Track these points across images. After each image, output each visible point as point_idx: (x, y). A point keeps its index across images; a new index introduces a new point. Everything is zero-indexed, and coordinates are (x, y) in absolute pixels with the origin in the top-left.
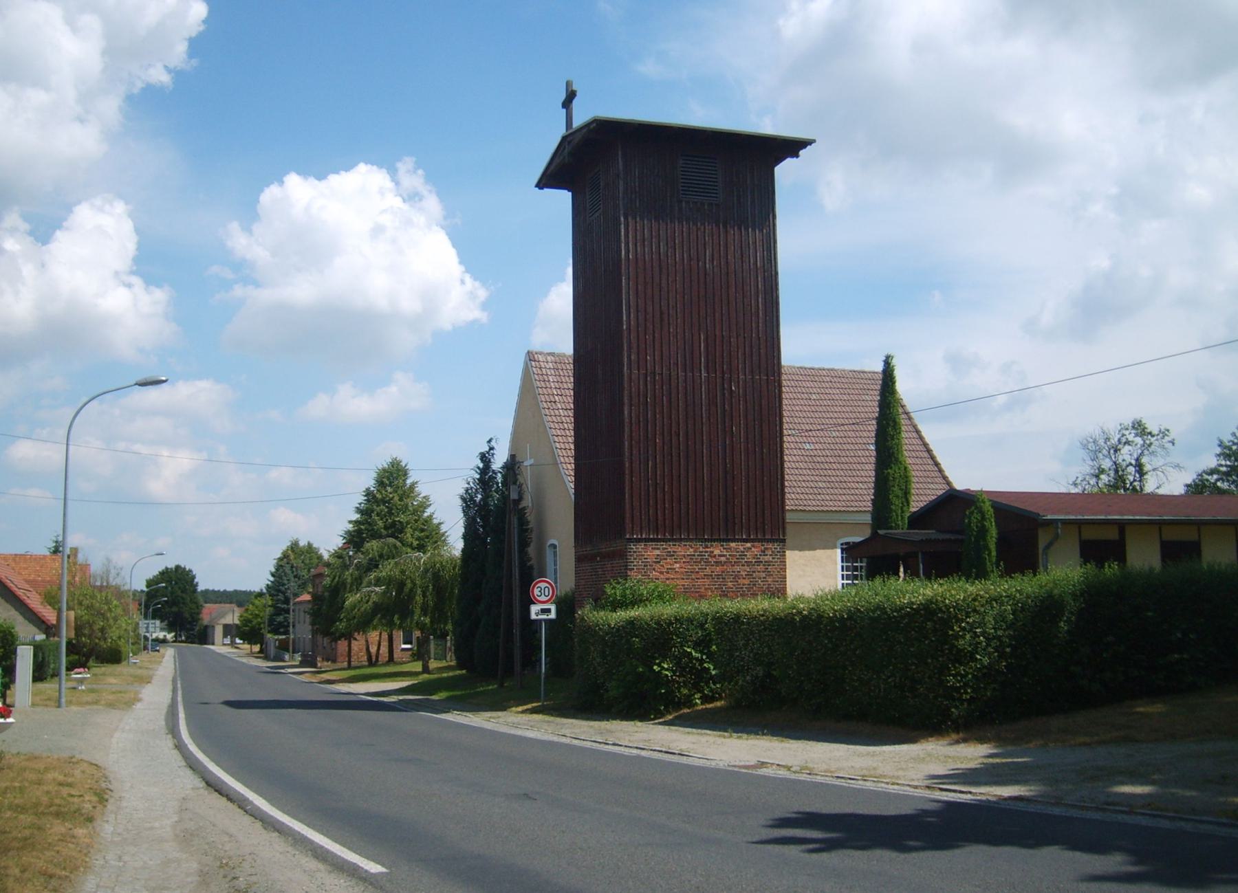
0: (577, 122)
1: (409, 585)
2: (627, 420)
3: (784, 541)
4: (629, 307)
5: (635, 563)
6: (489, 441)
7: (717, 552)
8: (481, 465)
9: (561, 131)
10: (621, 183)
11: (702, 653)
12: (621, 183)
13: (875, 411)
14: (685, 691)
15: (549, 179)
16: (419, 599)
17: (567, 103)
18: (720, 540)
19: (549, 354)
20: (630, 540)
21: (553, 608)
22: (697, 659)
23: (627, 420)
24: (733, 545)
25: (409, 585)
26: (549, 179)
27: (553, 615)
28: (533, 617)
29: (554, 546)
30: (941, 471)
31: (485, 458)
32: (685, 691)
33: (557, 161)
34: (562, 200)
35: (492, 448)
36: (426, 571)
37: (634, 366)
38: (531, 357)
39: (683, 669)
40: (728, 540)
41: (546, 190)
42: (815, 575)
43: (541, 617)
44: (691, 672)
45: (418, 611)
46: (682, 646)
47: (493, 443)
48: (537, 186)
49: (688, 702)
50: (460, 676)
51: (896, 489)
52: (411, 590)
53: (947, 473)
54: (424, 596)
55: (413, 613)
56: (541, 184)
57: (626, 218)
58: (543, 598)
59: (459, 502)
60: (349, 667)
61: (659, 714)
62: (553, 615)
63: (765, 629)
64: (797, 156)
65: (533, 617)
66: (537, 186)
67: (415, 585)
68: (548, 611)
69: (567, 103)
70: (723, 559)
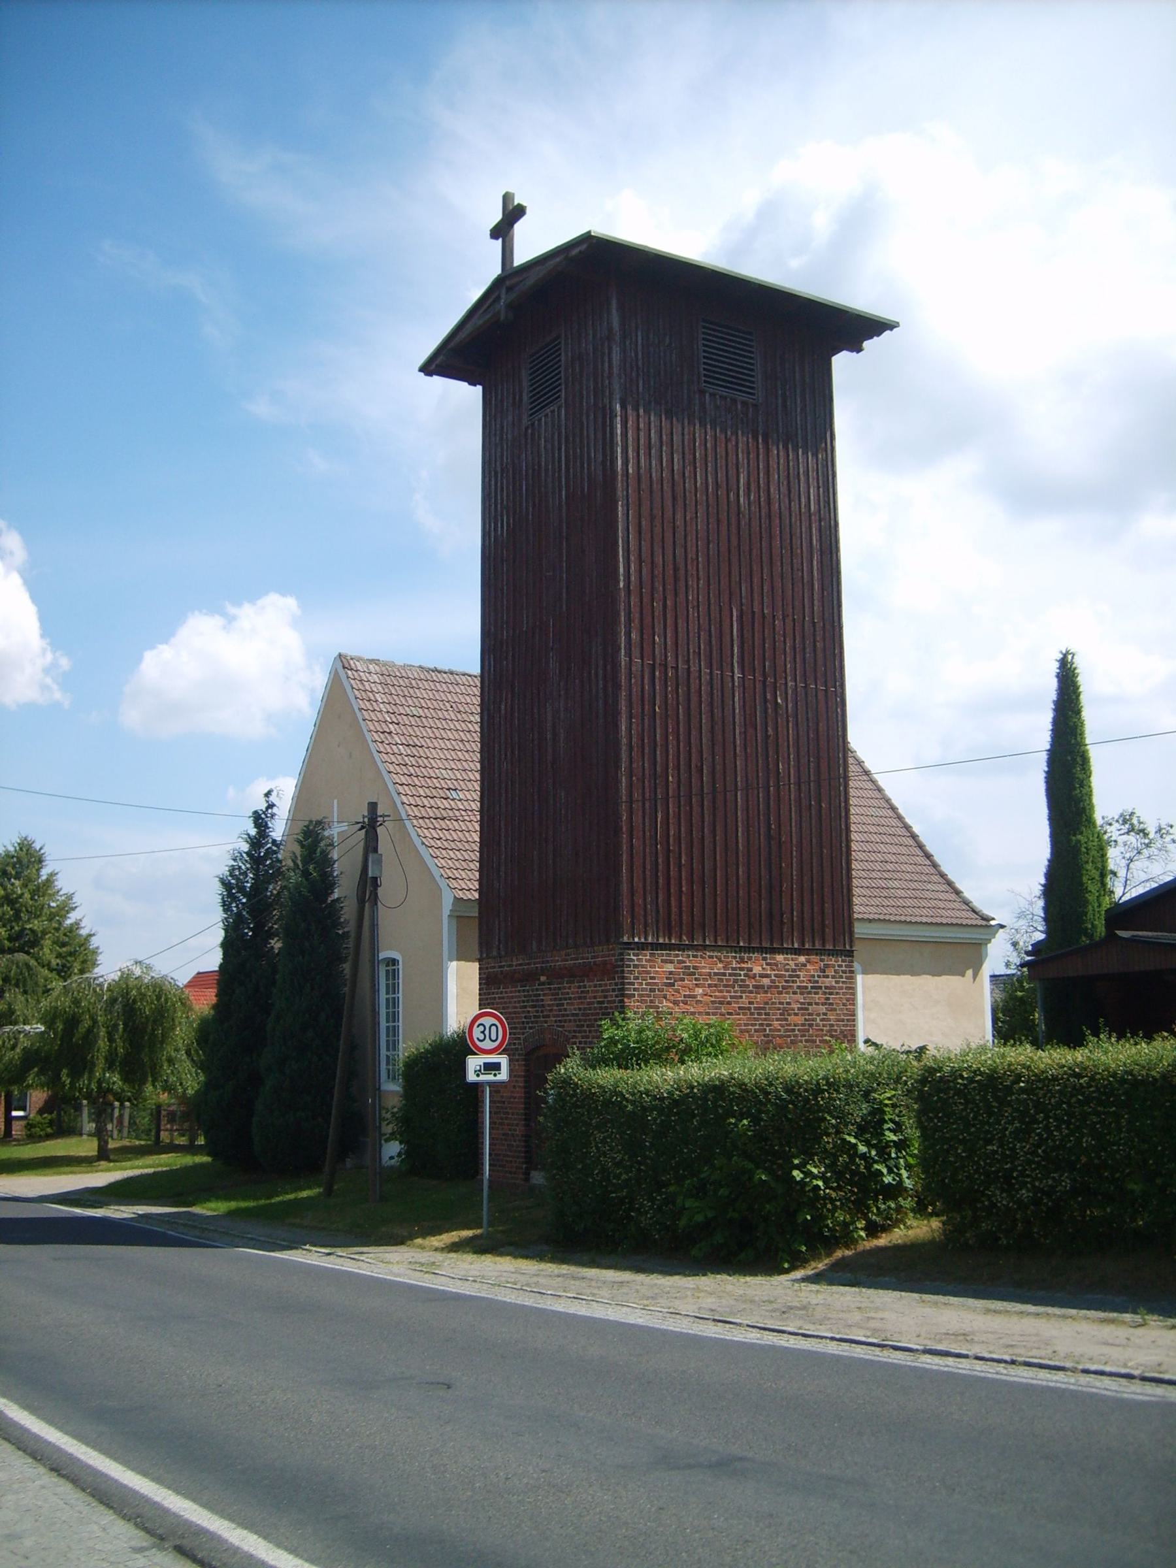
0: (521, 257)
1: (87, 1023)
2: (624, 741)
3: (850, 954)
4: (627, 551)
5: (637, 985)
6: (268, 794)
7: (757, 970)
8: (253, 832)
9: (494, 270)
10: (616, 350)
11: (868, 1143)
12: (616, 350)
13: (1043, 739)
14: (841, 1216)
15: (447, 361)
16: (103, 1044)
17: (503, 231)
18: (762, 950)
19: (372, 661)
20: (629, 946)
21: (503, 1060)
22: (863, 1156)
23: (624, 741)
24: (780, 958)
25: (87, 1023)
26: (447, 361)
27: (503, 1075)
28: (471, 1077)
29: (394, 962)
30: (935, 865)
31: (261, 821)
32: (841, 1216)
33: (477, 321)
34: (465, 399)
35: (271, 806)
36: (113, 1001)
37: (636, 652)
38: (343, 662)
39: (839, 1175)
40: (773, 951)
41: (435, 377)
42: (923, 1017)
43: (483, 1078)
44: (851, 1182)
45: (101, 1063)
46: (838, 1132)
47: (273, 798)
48: (422, 369)
49: (845, 1237)
50: (202, 1165)
51: (1089, 866)
52: (90, 1031)
53: (944, 869)
54: (111, 1040)
55: (93, 1064)
56: (429, 368)
57: (624, 407)
58: (487, 1045)
59: (217, 889)
60: (104, 1154)
61: (798, 1261)
62: (503, 1075)
63: (1087, 1101)
64: (859, 349)
65: (471, 1077)
66: (422, 369)
67: (95, 1022)
68: (495, 1067)
69: (503, 231)
70: (766, 981)
